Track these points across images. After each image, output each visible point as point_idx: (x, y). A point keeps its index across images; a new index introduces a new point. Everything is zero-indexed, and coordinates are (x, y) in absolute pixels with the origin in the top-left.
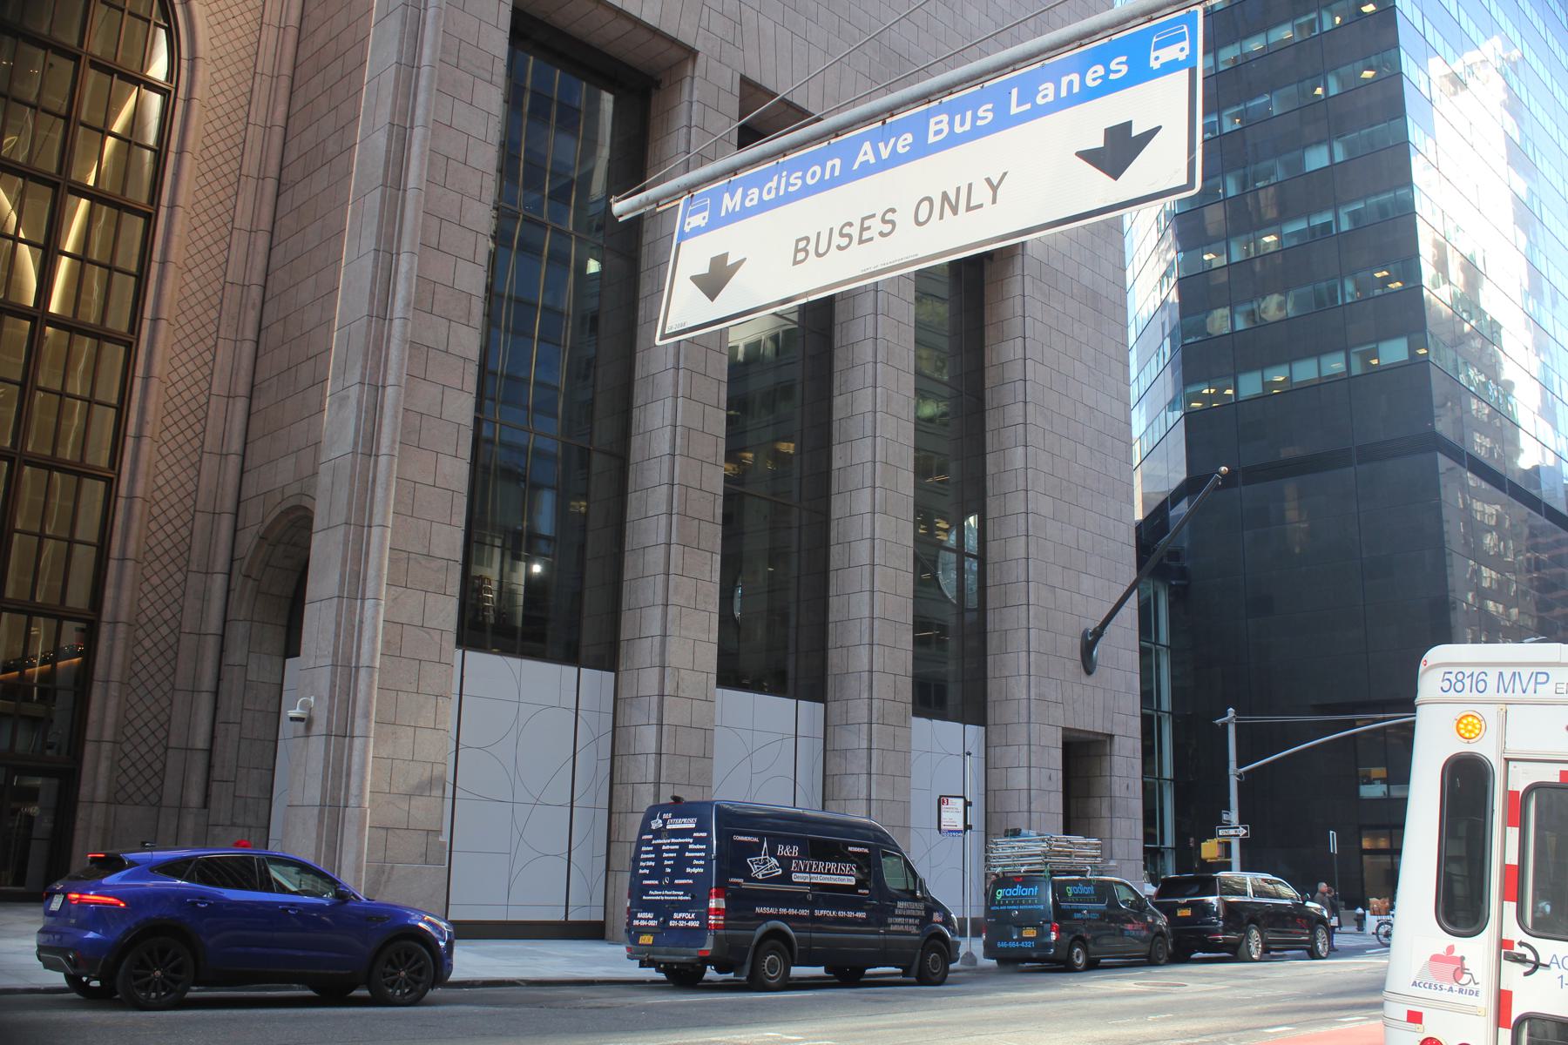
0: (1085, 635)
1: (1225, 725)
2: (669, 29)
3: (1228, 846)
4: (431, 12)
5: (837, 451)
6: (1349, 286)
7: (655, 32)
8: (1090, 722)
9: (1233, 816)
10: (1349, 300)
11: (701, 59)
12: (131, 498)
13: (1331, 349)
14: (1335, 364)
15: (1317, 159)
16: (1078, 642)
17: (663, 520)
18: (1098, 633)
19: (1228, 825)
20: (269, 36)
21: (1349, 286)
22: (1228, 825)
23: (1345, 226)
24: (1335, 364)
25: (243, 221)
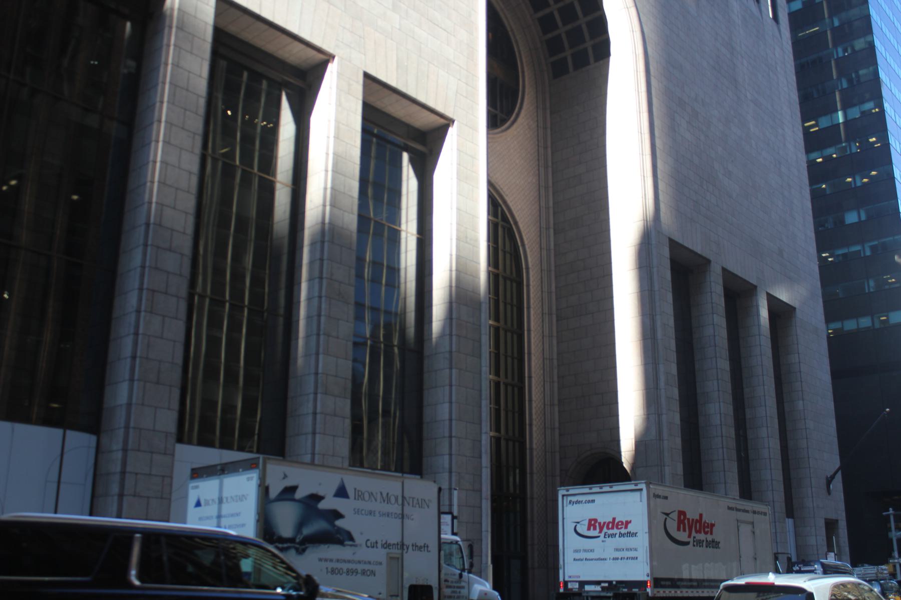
0: (827, 477)
1: (889, 516)
2: (704, 255)
3: (894, 566)
4: (655, 270)
5: (748, 411)
6: (872, 283)
7: (700, 256)
8: (833, 516)
9: (896, 554)
10: (872, 290)
11: (712, 263)
12: (531, 449)
13: (864, 315)
14: (865, 322)
15: (851, 218)
16: (825, 481)
17: (720, 451)
18: (833, 477)
19: (894, 558)
20: (544, 253)
21: (872, 283)
22: (894, 558)
23: (868, 253)
24: (865, 322)
25: (546, 333)
